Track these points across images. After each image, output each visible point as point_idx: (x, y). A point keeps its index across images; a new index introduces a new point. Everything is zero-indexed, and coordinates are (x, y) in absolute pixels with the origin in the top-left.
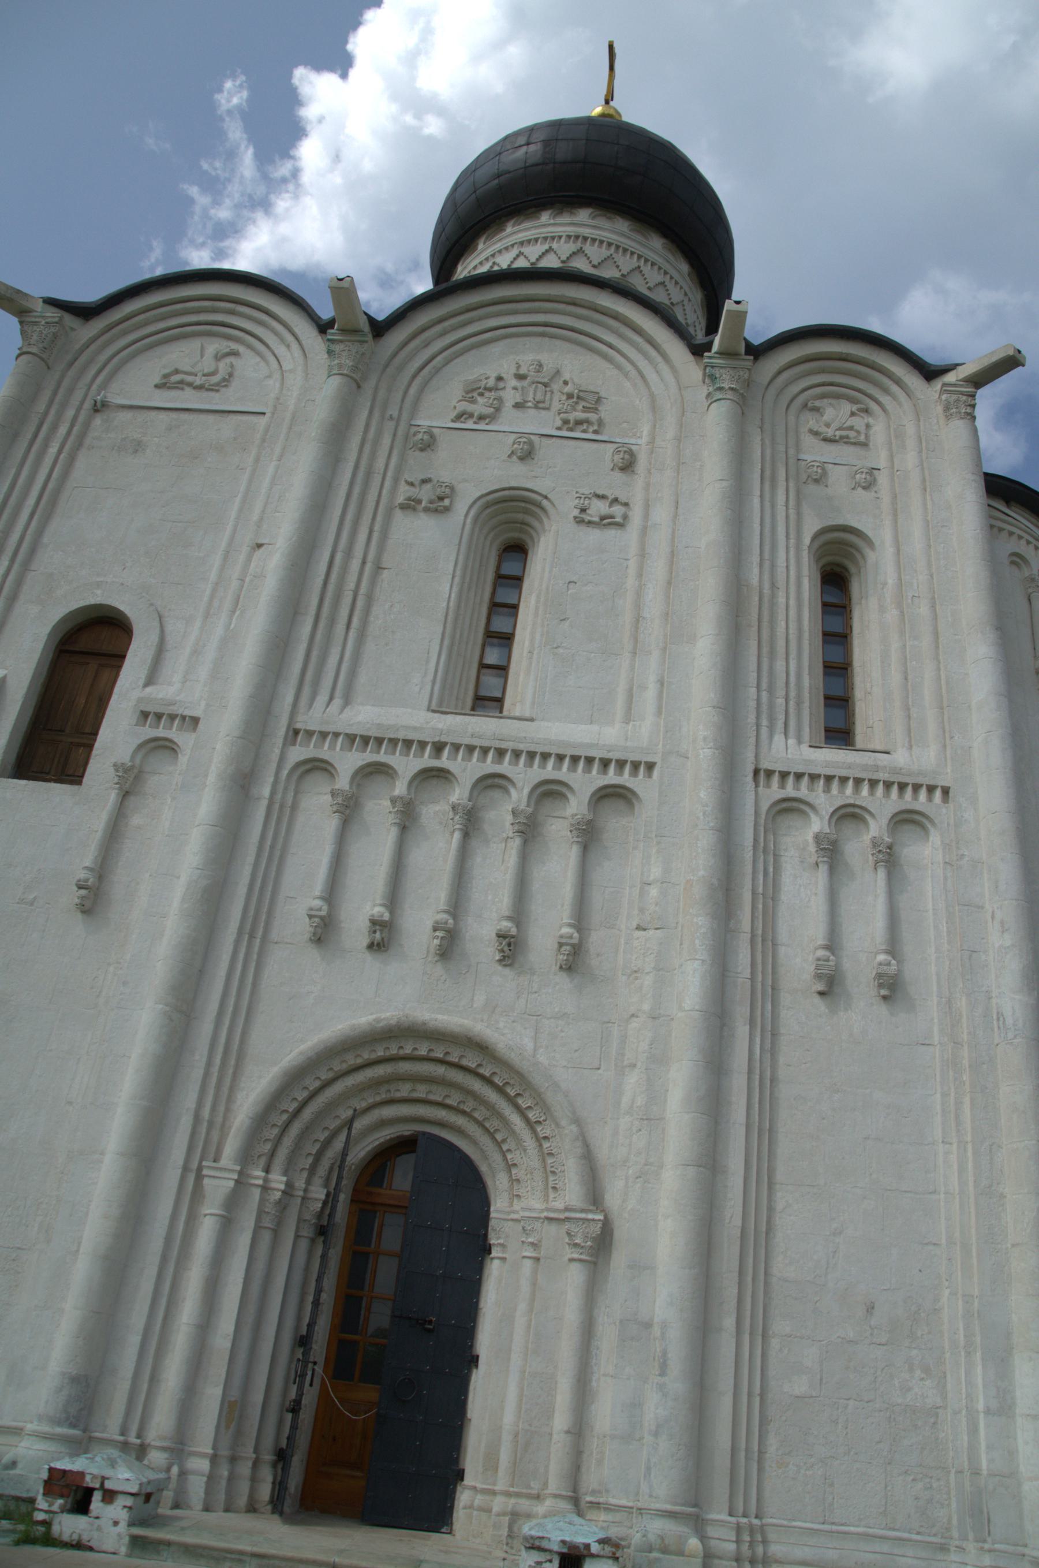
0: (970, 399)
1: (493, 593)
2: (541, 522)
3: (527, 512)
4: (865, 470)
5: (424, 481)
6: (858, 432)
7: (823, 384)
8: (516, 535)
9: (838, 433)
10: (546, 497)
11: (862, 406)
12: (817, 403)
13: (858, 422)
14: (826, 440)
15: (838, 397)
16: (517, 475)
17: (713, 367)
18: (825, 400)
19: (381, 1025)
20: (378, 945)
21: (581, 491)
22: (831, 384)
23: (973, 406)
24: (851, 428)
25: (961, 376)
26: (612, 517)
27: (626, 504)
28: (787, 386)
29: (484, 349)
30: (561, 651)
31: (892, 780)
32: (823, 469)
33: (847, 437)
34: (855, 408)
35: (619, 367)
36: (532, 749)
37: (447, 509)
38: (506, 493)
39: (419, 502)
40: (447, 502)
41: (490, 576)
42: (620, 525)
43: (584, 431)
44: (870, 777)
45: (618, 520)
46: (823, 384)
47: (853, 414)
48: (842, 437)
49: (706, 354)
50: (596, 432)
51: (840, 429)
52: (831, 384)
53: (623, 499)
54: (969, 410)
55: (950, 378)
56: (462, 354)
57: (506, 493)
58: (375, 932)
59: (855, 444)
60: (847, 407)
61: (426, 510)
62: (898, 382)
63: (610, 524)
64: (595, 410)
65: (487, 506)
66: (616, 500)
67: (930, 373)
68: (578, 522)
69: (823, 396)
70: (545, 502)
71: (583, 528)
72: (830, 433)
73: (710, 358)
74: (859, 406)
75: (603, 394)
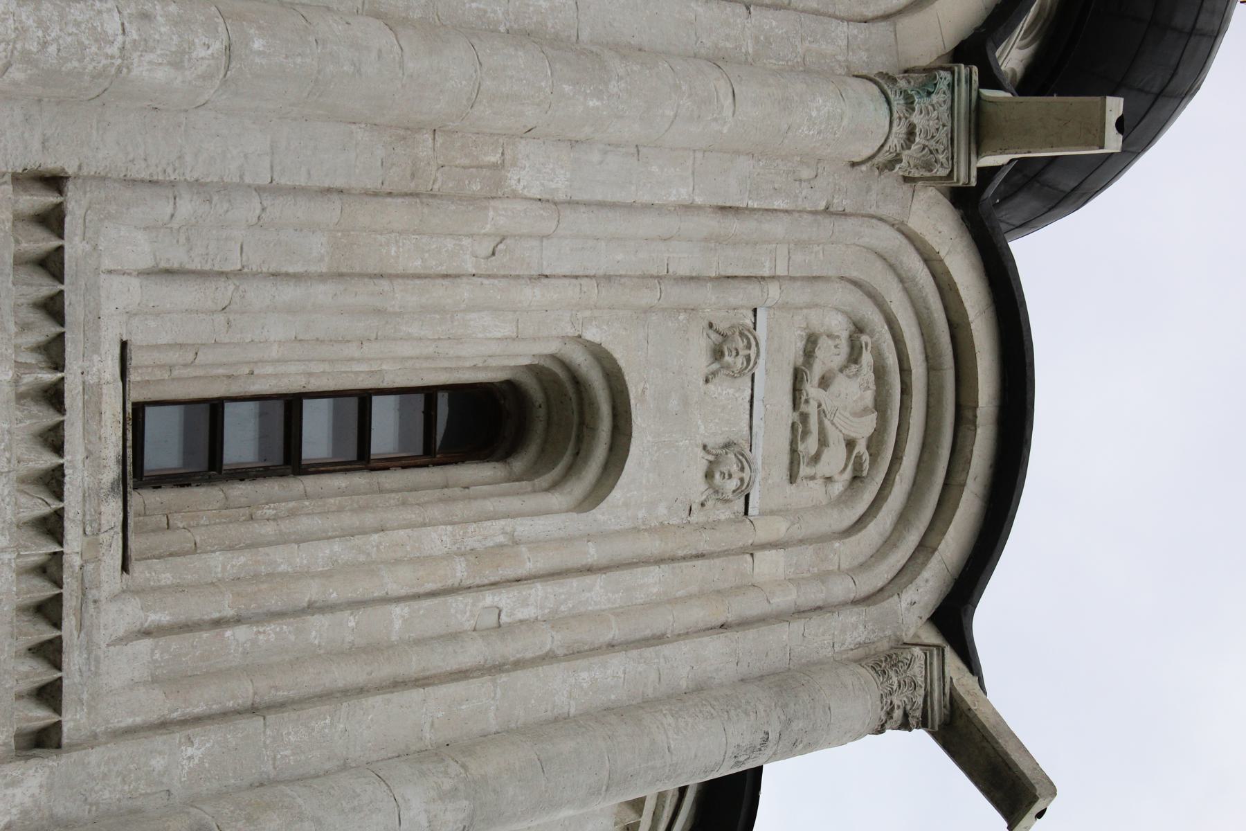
0: (918, 713)
4: (746, 475)
6: (816, 458)
7: (905, 371)
9: (812, 409)
11: (866, 466)
12: (867, 358)
13: (835, 460)
14: (798, 378)
15: (880, 406)
17: (951, 86)
18: (872, 377)
22: (906, 390)
23: (905, 725)
24: (823, 442)
25: (961, 690)
28: (901, 280)
31: (67, 578)
32: (741, 372)
33: (806, 433)
34: (861, 448)
44: (69, 515)
46: (905, 371)
47: (850, 444)
48: (804, 418)
49: (975, 69)
51: (822, 413)
52: (906, 390)
54: (898, 714)
55: (953, 663)
59: (794, 451)
60: (864, 427)
62: (925, 548)
67: (952, 619)
69: (880, 372)
72: (811, 389)
73: (969, 80)
74: (866, 457)
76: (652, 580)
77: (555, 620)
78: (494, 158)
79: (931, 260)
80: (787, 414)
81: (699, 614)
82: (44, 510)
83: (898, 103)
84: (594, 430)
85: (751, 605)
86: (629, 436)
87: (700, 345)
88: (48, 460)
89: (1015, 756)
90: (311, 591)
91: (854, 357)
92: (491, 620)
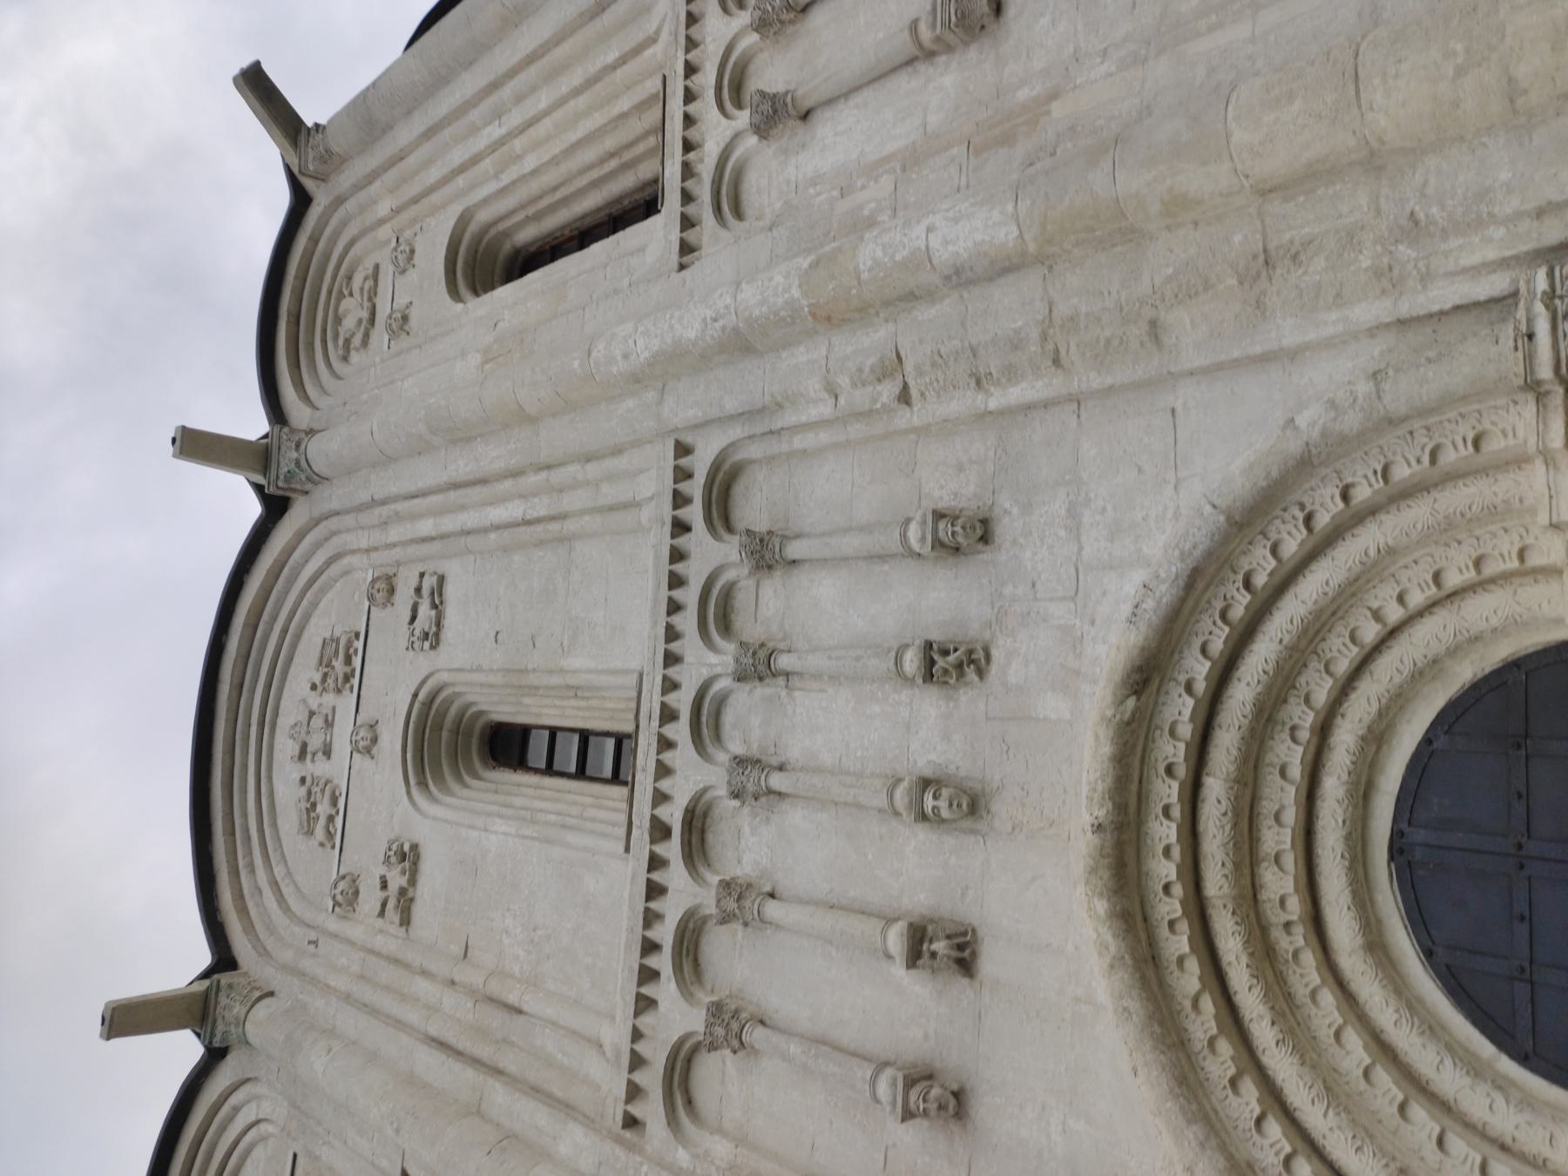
1: (536, 771)
2: (448, 702)
3: (439, 727)
5: (384, 885)
7: (324, 341)
8: (475, 741)
10: (415, 695)
16: (391, 739)
19: (1109, 938)
20: (961, 947)
21: (406, 644)
22: (324, 331)
24: (362, 289)
26: (432, 594)
27: (422, 575)
29: (278, 810)
30: (566, 643)
35: (307, 617)
36: (660, 658)
37: (414, 847)
38: (409, 756)
39: (402, 891)
40: (406, 848)
41: (548, 781)
42: (442, 580)
43: (356, 651)
45: (434, 579)
46: (324, 341)
48: (370, 299)
50: (357, 635)
53: (414, 582)
56: (279, 840)
57: (409, 756)
58: (933, 955)
59: (376, 281)
61: (413, 881)
63: (441, 595)
64: (338, 641)
65: (423, 784)
66: (418, 590)
67: (301, 200)
68: (438, 643)
70: (421, 696)
71: (443, 636)
75: (328, 635)
76: (434, 174)
77: (474, 130)
78: (487, 367)
79: (305, 398)
80: (378, 301)
81: (412, 160)
82: (694, 78)
83: (303, 464)
84: (466, 263)
85: (391, 176)
86: (446, 258)
87: (414, 322)
88: (691, 108)
89: (257, 105)
90: (581, 102)
91: (347, 341)
92: (504, 119)
